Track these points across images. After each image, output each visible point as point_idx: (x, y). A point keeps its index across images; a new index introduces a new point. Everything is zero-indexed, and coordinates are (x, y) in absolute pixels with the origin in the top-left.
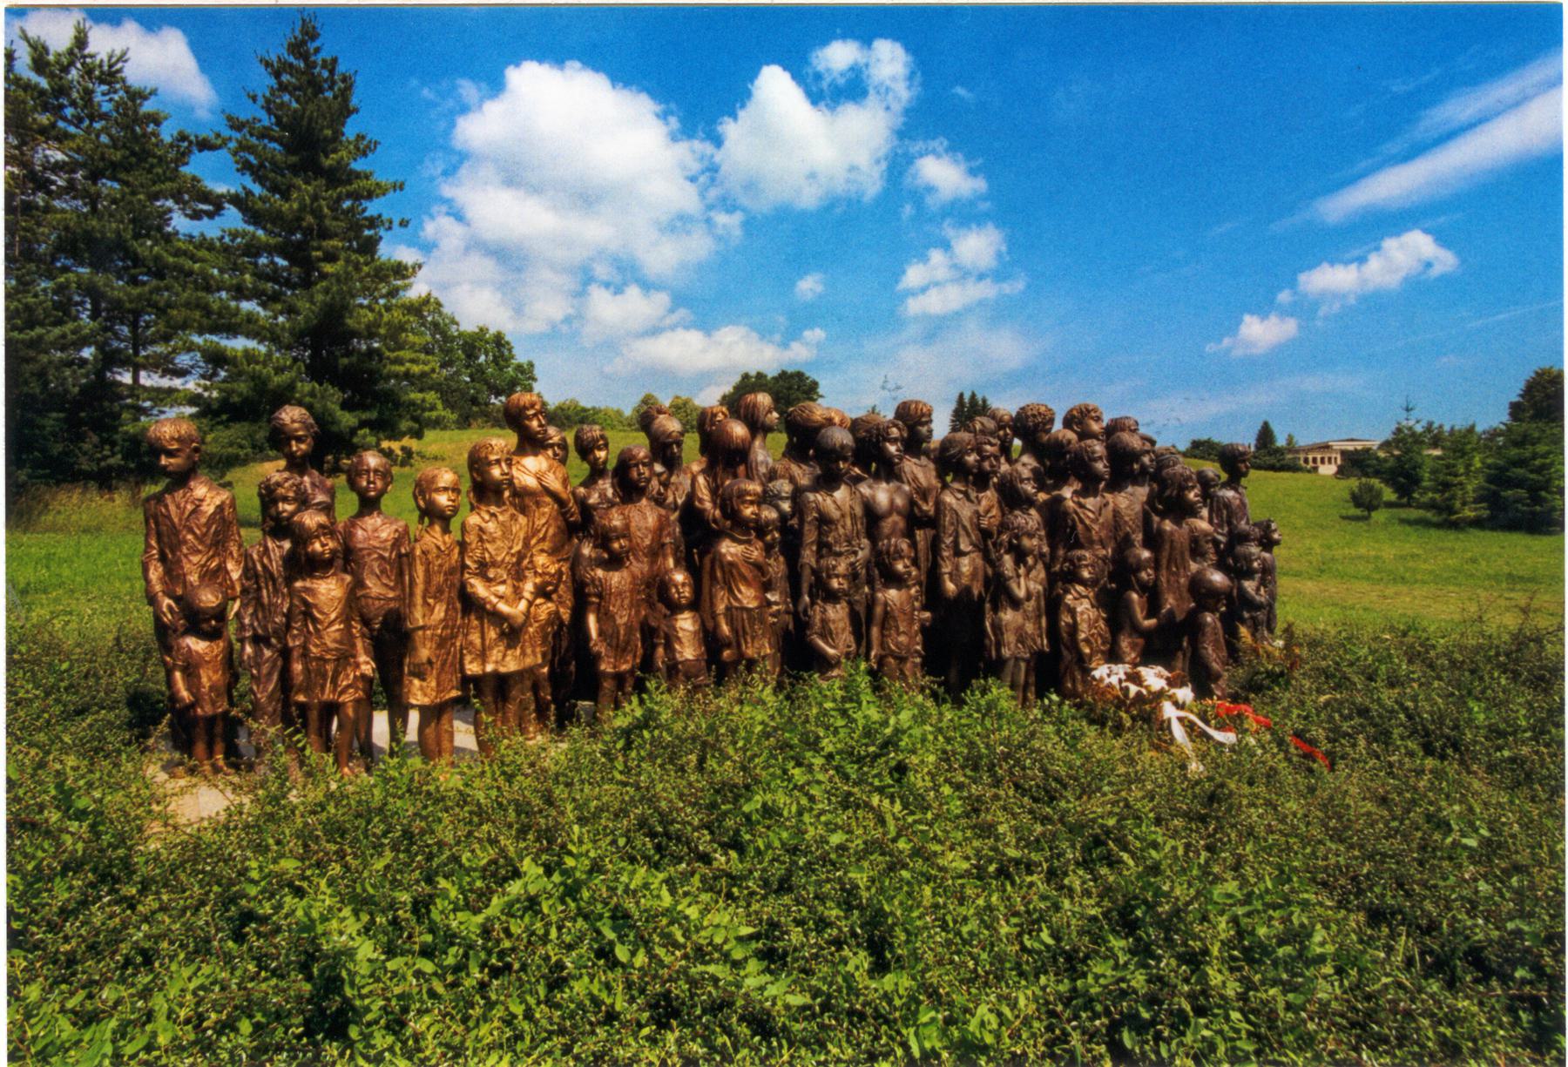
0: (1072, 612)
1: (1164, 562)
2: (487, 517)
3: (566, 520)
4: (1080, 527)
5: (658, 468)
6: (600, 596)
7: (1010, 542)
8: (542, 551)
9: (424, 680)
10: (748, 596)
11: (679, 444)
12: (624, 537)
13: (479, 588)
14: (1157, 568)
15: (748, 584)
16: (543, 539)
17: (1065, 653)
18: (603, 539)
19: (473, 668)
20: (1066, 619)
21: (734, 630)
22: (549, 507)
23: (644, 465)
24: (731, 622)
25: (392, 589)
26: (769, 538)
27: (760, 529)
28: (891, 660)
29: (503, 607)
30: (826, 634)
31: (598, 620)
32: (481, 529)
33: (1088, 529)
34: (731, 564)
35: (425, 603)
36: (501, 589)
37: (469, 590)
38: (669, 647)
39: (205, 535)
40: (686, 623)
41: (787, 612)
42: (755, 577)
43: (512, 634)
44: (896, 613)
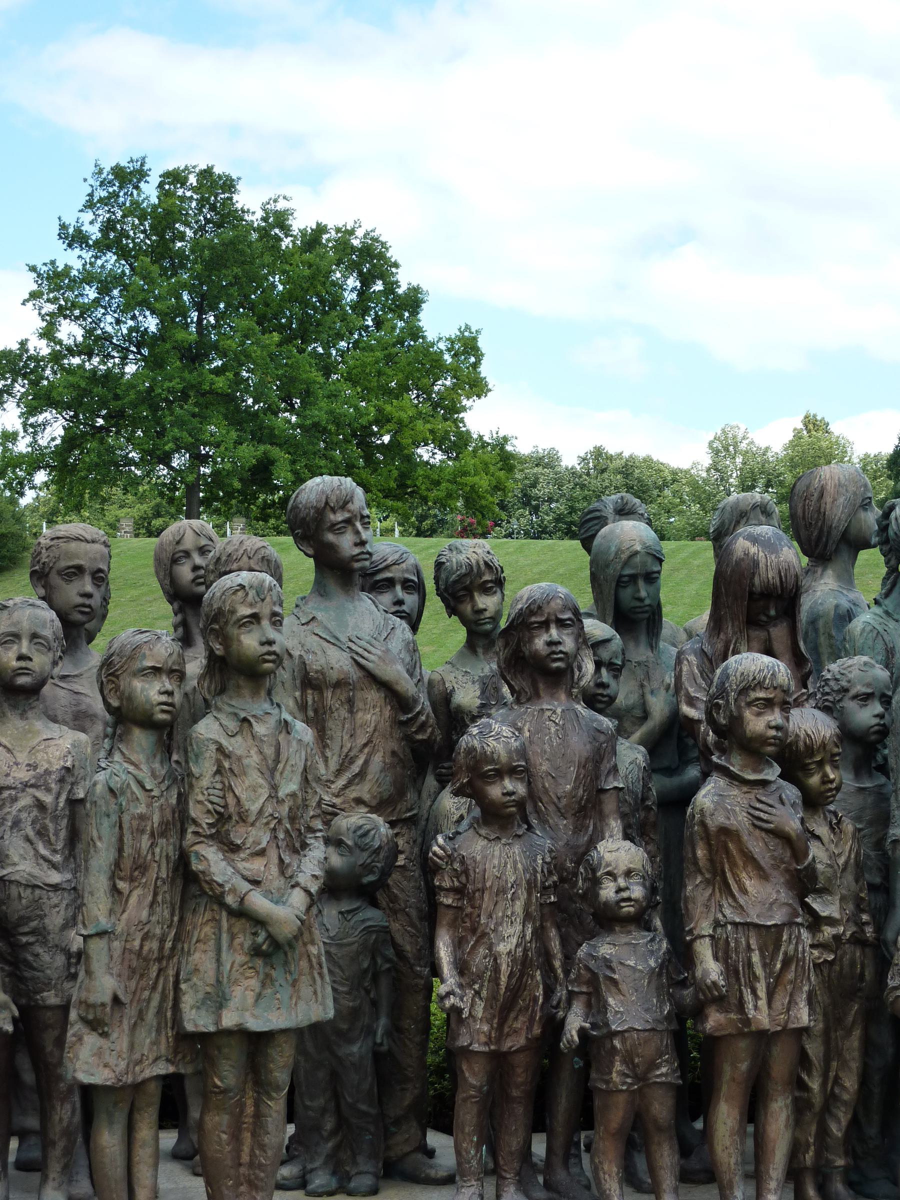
2: (232, 725)
3: (408, 738)
5: (596, 628)
6: (460, 891)
8: (359, 801)
9: (105, 1035)
10: (762, 898)
11: (651, 578)
12: (512, 771)
13: (212, 861)
15: (763, 875)
16: (361, 775)
18: (476, 777)
19: (197, 1020)
21: (731, 971)
22: (373, 713)
23: (561, 624)
24: (722, 953)
25: (54, 866)
26: (814, 780)
29: (259, 902)
31: (458, 944)
32: (220, 749)
34: (724, 831)
35: (115, 890)
36: (256, 866)
37: (196, 866)
38: (596, 1004)
40: (629, 956)
41: (858, 940)
42: (778, 862)
43: (272, 951)
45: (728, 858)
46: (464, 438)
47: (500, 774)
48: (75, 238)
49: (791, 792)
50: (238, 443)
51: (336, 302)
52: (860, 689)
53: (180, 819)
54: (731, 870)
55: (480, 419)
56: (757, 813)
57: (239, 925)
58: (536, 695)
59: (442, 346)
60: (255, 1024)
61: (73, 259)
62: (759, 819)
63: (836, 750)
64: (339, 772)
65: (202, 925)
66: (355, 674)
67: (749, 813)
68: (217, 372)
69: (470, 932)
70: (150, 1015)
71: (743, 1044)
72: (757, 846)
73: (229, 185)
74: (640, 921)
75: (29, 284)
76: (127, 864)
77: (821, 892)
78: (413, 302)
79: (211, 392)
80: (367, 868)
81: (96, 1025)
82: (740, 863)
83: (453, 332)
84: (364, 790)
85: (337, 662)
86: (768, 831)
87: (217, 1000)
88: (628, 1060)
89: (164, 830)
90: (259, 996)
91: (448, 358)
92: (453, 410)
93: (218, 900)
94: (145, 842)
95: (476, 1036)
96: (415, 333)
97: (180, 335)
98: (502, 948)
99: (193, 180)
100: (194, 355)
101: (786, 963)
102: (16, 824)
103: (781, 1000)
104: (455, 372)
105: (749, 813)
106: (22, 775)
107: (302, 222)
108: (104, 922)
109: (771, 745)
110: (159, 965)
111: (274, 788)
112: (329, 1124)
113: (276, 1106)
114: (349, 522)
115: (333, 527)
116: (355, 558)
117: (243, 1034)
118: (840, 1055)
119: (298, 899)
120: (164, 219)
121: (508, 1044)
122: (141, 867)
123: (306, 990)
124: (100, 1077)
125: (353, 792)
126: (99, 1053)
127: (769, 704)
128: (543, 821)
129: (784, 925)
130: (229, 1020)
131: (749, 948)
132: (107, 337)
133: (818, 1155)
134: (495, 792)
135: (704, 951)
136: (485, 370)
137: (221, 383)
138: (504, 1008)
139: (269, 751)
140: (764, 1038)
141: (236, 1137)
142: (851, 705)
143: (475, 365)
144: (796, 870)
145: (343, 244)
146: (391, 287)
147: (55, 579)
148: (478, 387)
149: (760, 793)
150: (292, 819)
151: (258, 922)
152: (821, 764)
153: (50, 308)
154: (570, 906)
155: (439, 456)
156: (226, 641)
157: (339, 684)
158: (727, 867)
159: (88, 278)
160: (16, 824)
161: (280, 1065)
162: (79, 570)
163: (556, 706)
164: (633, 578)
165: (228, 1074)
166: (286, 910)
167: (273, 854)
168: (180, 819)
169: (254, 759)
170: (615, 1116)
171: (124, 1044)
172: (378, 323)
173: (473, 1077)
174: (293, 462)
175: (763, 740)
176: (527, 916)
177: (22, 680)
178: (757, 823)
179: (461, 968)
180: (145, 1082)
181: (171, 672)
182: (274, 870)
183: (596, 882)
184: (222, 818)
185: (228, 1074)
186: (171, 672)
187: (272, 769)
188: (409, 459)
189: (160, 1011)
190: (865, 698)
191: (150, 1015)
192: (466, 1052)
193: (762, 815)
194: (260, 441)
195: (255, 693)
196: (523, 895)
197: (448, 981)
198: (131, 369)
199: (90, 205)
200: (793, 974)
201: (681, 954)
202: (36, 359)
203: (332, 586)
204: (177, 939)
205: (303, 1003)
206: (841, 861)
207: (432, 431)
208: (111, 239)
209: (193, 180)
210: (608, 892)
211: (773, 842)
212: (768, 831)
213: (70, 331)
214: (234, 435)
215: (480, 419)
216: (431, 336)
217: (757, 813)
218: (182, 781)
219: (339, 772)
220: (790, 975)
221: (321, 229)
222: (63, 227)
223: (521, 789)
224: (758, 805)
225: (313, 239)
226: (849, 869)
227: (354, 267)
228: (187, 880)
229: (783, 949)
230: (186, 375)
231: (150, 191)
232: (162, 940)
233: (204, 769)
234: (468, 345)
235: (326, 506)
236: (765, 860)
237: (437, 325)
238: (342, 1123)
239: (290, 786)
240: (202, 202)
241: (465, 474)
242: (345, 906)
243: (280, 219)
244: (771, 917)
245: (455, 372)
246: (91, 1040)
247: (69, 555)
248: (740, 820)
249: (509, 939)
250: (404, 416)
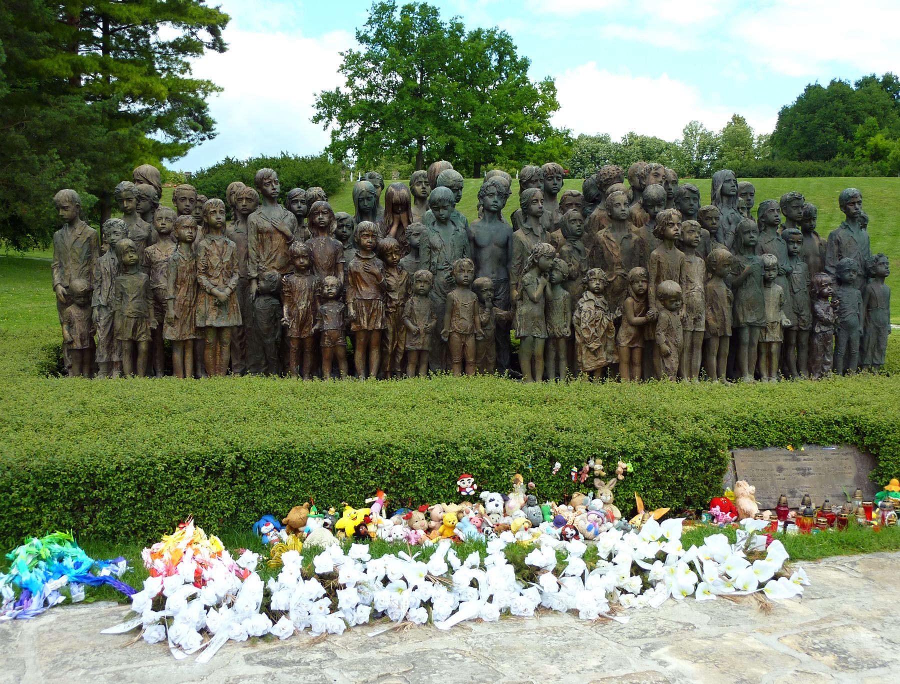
0: (580, 310)
1: (653, 278)
2: (210, 242)
4: (606, 252)
7: (533, 261)
8: (274, 268)
13: (203, 279)
14: (648, 282)
15: (367, 285)
16: (274, 260)
17: (577, 337)
19: (200, 323)
20: (576, 314)
21: (357, 313)
22: (278, 240)
23: (323, 213)
26: (390, 259)
27: (381, 253)
28: (455, 335)
30: (411, 316)
33: (611, 254)
34: (356, 273)
35: (175, 287)
36: (216, 281)
39: (81, 254)
40: (332, 309)
42: (372, 281)
43: (221, 305)
44: (459, 306)
46: (549, 131)
47: (299, 257)
48: (363, 39)
49: (379, 261)
50: (438, 135)
51: (485, 65)
52: (415, 232)
53: (195, 269)
55: (557, 121)
57: (211, 298)
58: (318, 235)
59: (537, 86)
60: (215, 324)
61: (363, 49)
64: (267, 259)
65: (201, 297)
66: (272, 229)
68: (429, 101)
69: (293, 304)
70: (188, 322)
71: (362, 333)
72: (365, 277)
73: (435, 12)
74: (336, 298)
75: (341, 61)
76: (179, 281)
77: (392, 291)
78: (524, 65)
79: (425, 111)
80: (272, 287)
81: (170, 324)
83: (542, 80)
84: (275, 264)
85: (267, 225)
87: (205, 318)
88: (329, 338)
89: (191, 271)
90: (217, 318)
91: (540, 92)
92: (541, 117)
93: (205, 290)
94: (185, 274)
95: (293, 333)
96: (525, 80)
97: (410, 84)
98: (300, 308)
99: (417, 10)
100: (417, 93)
101: (374, 310)
102: (162, 272)
103: (372, 321)
104: (544, 99)
106: (164, 258)
107: (469, 28)
108: (172, 296)
110: (190, 308)
111: (222, 260)
112: (263, 363)
113: (226, 349)
114: (270, 182)
115: (266, 184)
116: (272, 194)
117: (211, 327)
118: (399, 339)
119: (228, 291)
120: (404, 29)
121: (302, 336)
122: (183, 281)
123: (232, 316)
124: (172, 338)
125: (272, 265)
126: (171, 331)
127: (368, 236)
128: (318, 272)
130: (208, 323)
132: (378, 86)
133: (391, 368)
134: (298, 262)
135: (351, 307)
136: (558, 98)
137: (430, 106)
138: (302, 325)
139: (221, 249)
140: (368, 333)
141: (215, 356)
142: (413, 237)
143: (553, 96)
145: (490, 38)
146: (514, 58)
147: (178, 201)
148: (555, 106)
149: (367, 261)
150: (227, 268)
151: (216, 296)
152: (391, 254)
153: (350, 72)
154: (319, 297)
155: (537, 140)
156: (208, 219)
157: (267, 232)
159: (368, 58)
160: (162, 272)
161: (226, 337)
162: (185, 198)
163: (323, 238)
164: (363, 199)
165: (210, 339)
166: (223, 294)
167: (221, 278)
168: (195, 269)
169: (216, 251)
170: (327, 354)
171: (179, 329)
172: (507, 75)
173: (294, 345)
174: (465, 144)
175: (367, 246)
176: (308, 299)
177: (163, 231)
178: (365, 270)
179: (289, 313)
180: (186, 340)
181: (192, 227)
182: (221, 282)
183: (323, 288)
184: (207, 268)
185: (210, 339)
186: (192, 227)
187: (221, 254)
188: (522, 141)
189: (190, 321)
190: (418, 234)
191: (188, 322)
192: (290, 338)
194: (449, 134)
195: (217, 233)
196: (307, 293)
197: (286, 317)
198: (389, 101)
199: (370, 22)
201: (346, 309)
202: (347, 96)
203: (267, 203)
204: (195, 302)
205: (233, 320)
207: (532, 128)
208: (380, 38)
209: (417, 10)
210: (326, 291)
211: (370, 276)
213: (361, 83)
214: (436, 131)
215: (557, 121)
216: (532, 81)
218: (195, 257)
219: (267, 259)
220: (375, 314)
221: (479, 32)
222: (358, 33)
223: (306, 262)
225: (476, 36)
227: (496, 49)
228: (198, 287)
230: (414, 103)
231: (397, 16)
232: (191, 302)
233: (201, 254)
234: (549, 86)
235: (263, 178)
236: (368, 281)
237: (535, 77)
238: (267, 363)
239: (227, 259)
240: (422, 20)
241: (548, 148)
242: (266, 298)
243: (459, 28)
245: (544, 99)
246: (169, 328)
247: (182, 194)
248: (360, 269)
249: (303, 305)
250: (518, 120)
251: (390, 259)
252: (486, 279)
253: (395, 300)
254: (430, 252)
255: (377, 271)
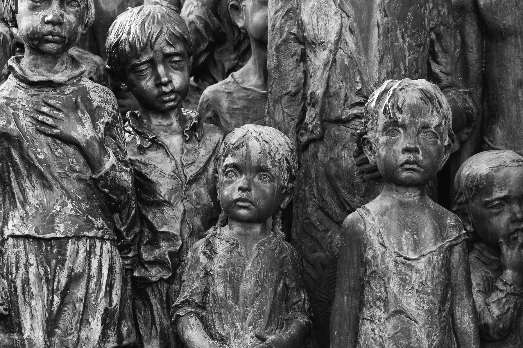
45: (13, 166)
54: (17, 179)
56: (40, 118)
62: (43, 123)
63: (169, 50)
67: (33, 117)
82: (24, 171)
86: (55, 137)
101: (73, 279)
105: (33, 117)
109: (48, 41)
129: (67, 238)
131: (27, 265)
144: (91, 178)
152: (152, 63)
158: (12, 175)
193: (46, 119)
200: (84, 292)
206: (191, 172)
212: (55, 137)
217: (40, 118)
224: (45, 109)
226: (203, 181)
229: (67, 264)
244: (53, 230)
251: (148, 84)
252: (507, 155)
253: (169, 237)
254: (303, 58)
255: (83, 131)
